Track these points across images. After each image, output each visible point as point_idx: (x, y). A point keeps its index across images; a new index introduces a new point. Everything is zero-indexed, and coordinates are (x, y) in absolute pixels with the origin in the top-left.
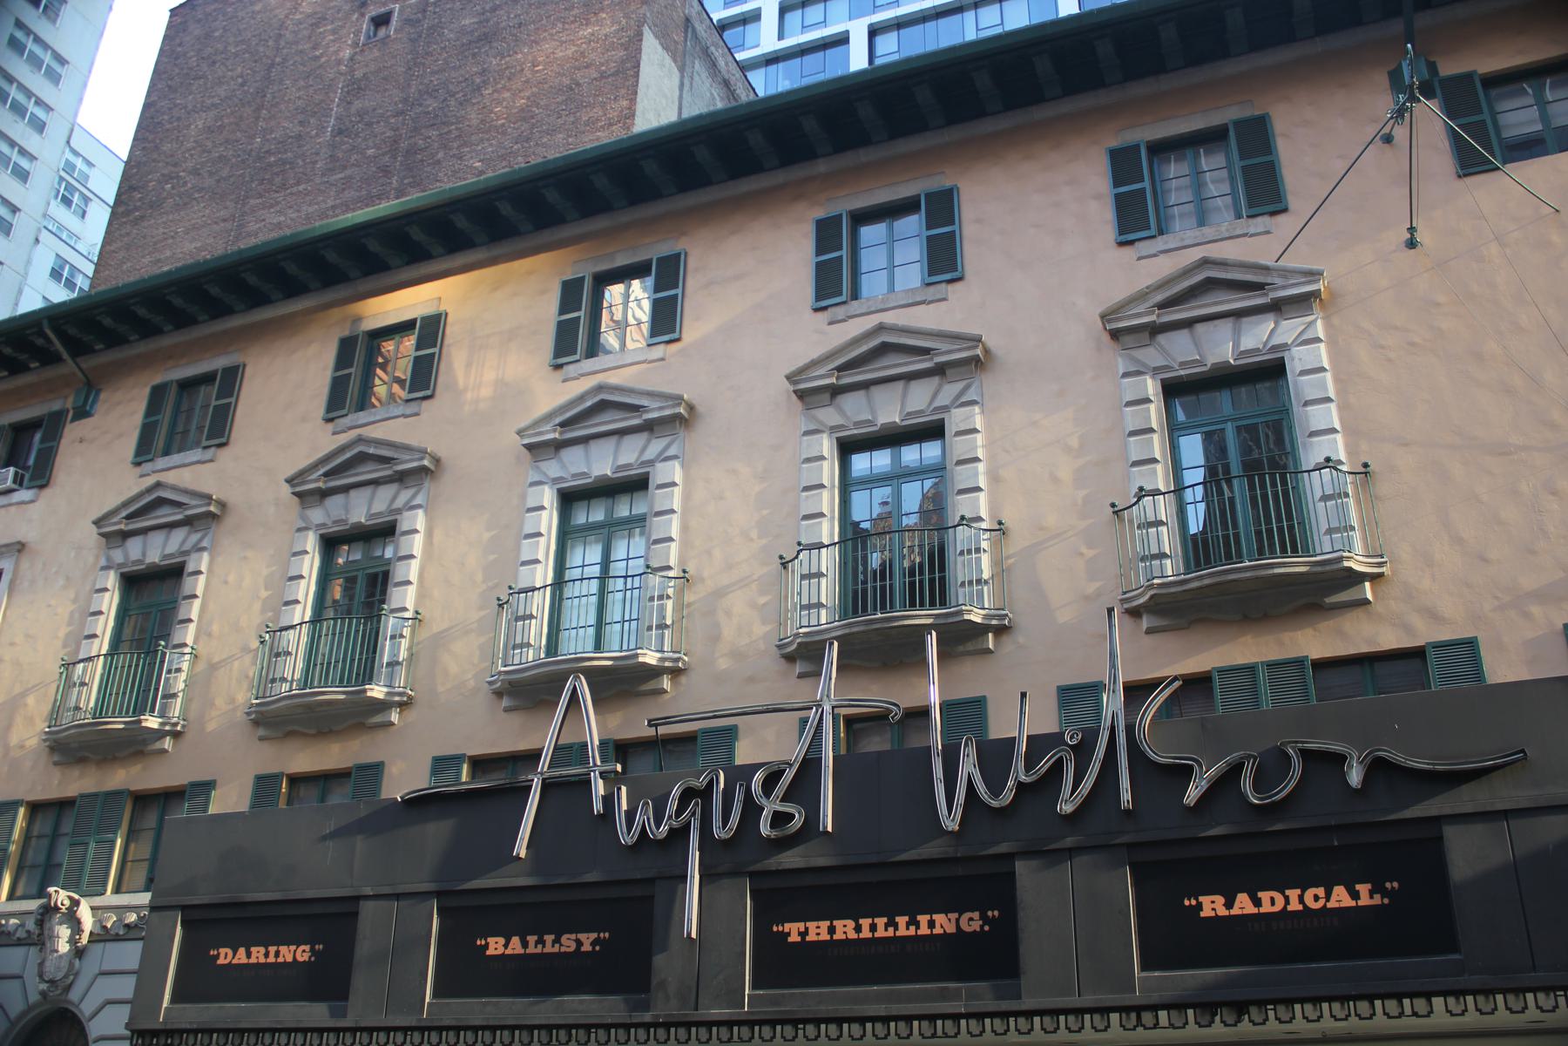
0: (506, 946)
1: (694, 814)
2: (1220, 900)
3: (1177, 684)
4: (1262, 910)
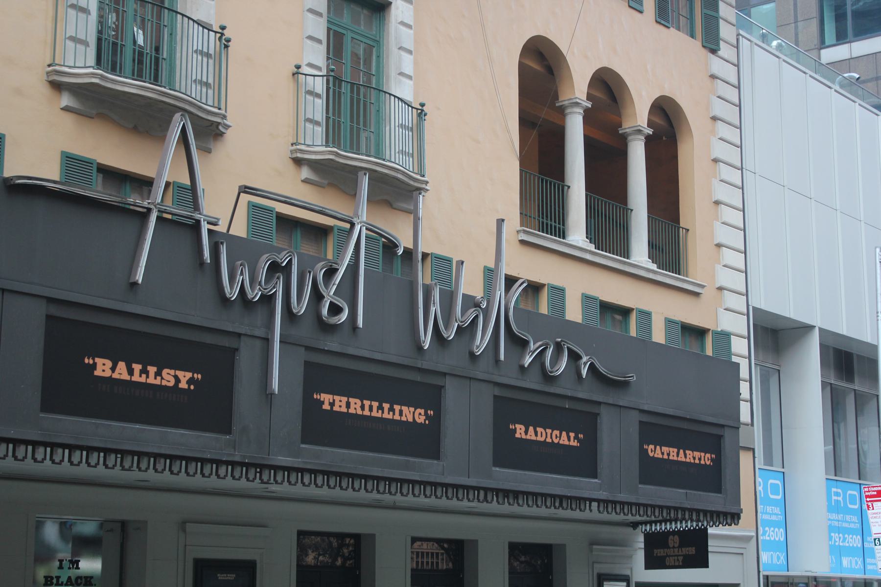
3: (525, 285)
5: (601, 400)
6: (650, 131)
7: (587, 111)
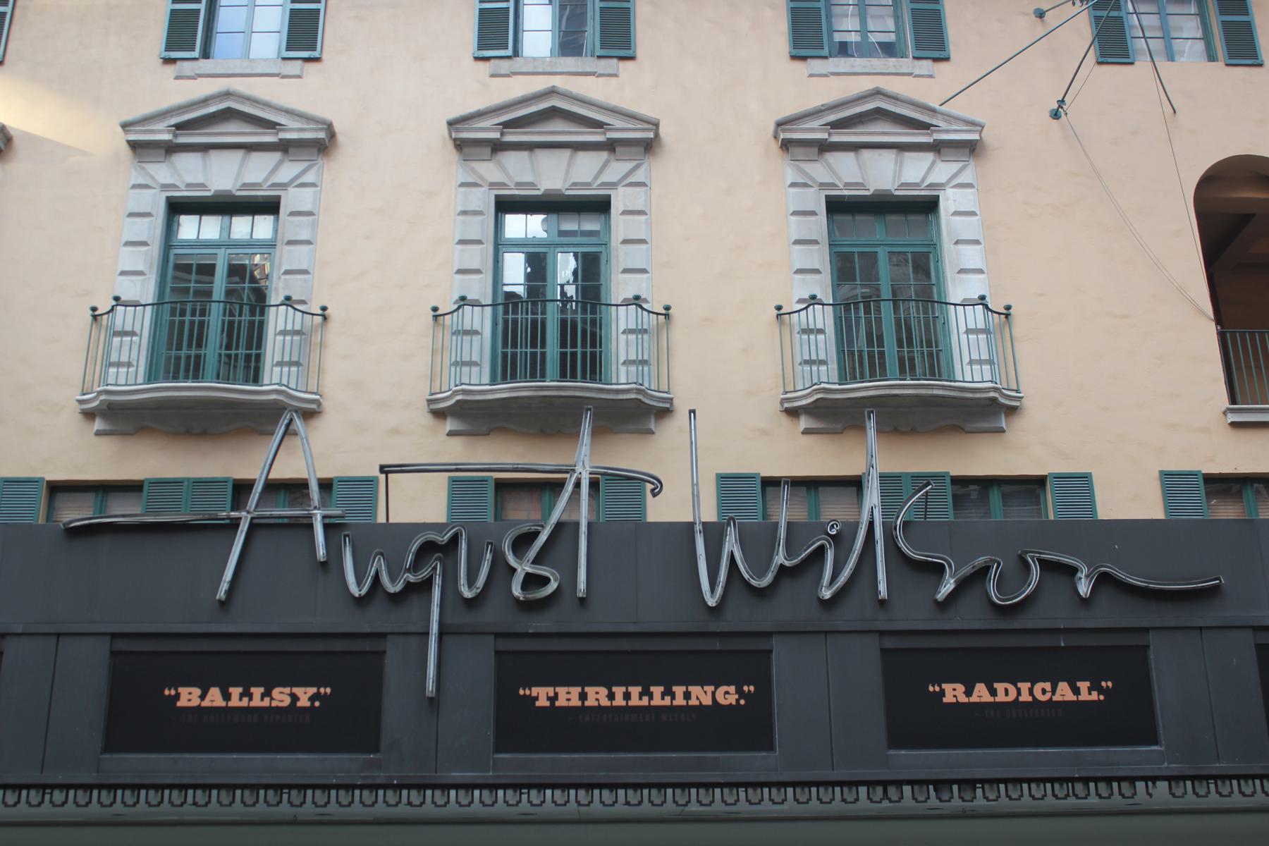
0: (202, 697)
1: (435, 568)
2: (960, 688)
4: (997, 699)
5: (1145, 624)
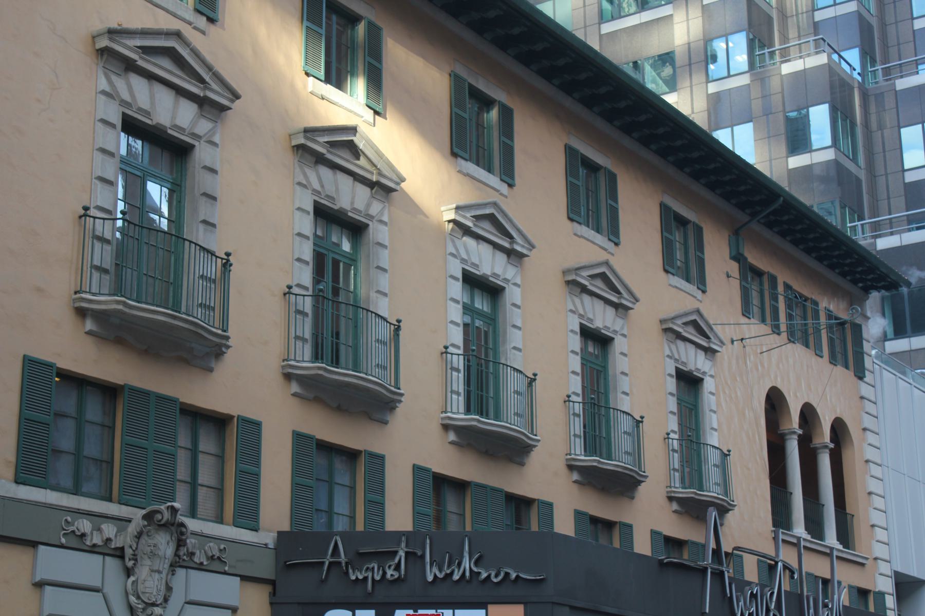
6: (800, 432)
7: (799, 436)
